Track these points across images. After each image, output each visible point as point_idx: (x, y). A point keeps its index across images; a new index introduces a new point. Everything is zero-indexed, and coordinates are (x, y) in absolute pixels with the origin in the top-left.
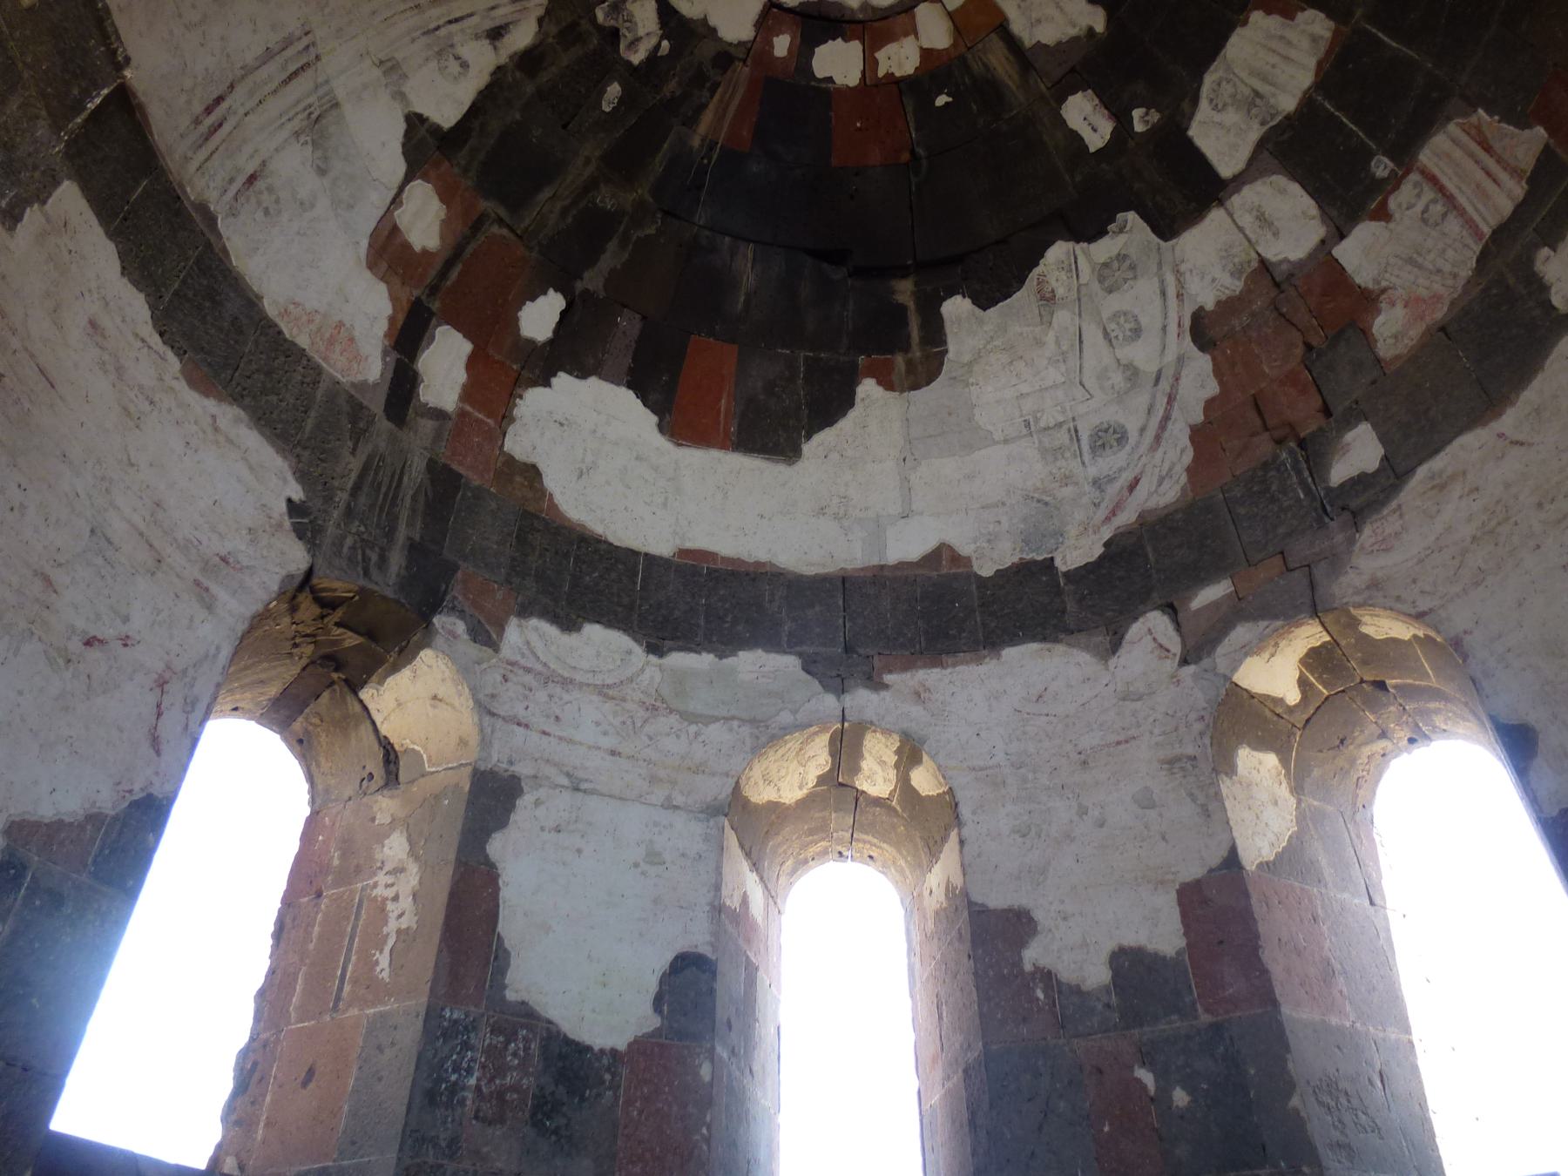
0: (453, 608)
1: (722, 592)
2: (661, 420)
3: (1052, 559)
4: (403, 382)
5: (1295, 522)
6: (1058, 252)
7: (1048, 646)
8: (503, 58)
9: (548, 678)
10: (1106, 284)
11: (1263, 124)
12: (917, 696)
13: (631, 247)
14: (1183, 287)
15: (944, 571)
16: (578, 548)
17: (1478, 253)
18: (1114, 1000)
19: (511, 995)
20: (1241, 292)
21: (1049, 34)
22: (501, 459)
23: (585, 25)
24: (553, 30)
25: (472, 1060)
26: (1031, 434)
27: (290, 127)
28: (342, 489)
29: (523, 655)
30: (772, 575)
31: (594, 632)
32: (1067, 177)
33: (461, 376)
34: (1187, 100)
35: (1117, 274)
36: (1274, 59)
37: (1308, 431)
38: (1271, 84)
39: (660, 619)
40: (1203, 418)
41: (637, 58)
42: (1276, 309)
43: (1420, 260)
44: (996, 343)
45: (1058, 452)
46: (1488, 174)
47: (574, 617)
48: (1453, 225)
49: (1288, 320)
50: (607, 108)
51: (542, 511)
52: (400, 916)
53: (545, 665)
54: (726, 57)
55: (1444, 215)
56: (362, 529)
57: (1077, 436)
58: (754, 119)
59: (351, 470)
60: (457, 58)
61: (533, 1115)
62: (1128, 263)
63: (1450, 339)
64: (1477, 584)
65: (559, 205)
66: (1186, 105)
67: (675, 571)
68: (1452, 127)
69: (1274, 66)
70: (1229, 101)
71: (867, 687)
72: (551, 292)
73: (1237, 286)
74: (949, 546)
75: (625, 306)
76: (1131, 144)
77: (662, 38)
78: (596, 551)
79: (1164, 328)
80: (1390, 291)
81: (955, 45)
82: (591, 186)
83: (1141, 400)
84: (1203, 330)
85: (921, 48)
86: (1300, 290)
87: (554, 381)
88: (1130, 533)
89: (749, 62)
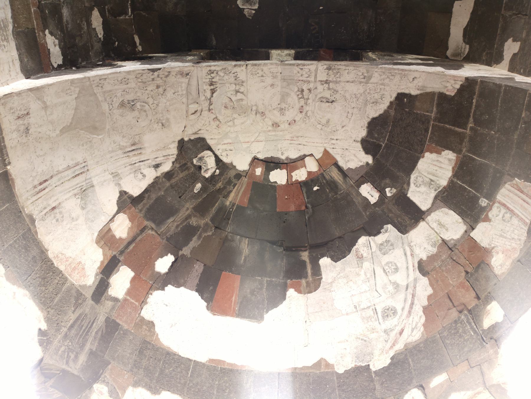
0: (104, 381)
1: (226, 379)
2: (208, 305)
3: (369, 365)
5: (471, 346)
6: (363, 240)
8: (159, 174)
10: (382, 252)
11: (435, 190)
13: (202, 239)
14: (413, 252)
15: (322, 371)
16: (165, 357)
17: (527, 230)
20: (436, 252)
23: (189, 164)
24: (178, 166)
26: (357, 311)
28: (65, 327)
30: (248, 371)
33: (128, 285)
34: (405, 184)
35: (386, 247)
37: (472, 306)
38: (436, 177)
39: (197, 390)
40: (427, 303)
41: (207, 175)
42: (452, 258)
43: (505, 235)
44: (342, 275)
45: (369, 318)
46: (524, 201)
47: (158, 388)
48: (515, 221)
49: (457, 262)
50: (196, 191)
51: (152, 341)
54: (239, 176)
55: (511, 218)
56: (70, 344)
57: (376, 312)
58: (249, 196)
59: (71, 319)
60: (142, 173)
63: (523, 264)
65: (176, 224)
66: (405, 186)
67: (206, 368)
68: (507, 185)
69: (436, 170)
70: (422, 183)
72: (169, 255)
73: (435, 250)
74: (325, 359)
75: (198, 261)
76: (386, 200)
77: (217, 169)
78: (173, 358)
79: (407, 268)
80: (495, 248)
81: (319, 170)
82: (189, 217)
83: (401, 296)
85: (307, 171)
86: (460, 250)
87: (166, 288)
88: (402, 353)
89: (247, 177)
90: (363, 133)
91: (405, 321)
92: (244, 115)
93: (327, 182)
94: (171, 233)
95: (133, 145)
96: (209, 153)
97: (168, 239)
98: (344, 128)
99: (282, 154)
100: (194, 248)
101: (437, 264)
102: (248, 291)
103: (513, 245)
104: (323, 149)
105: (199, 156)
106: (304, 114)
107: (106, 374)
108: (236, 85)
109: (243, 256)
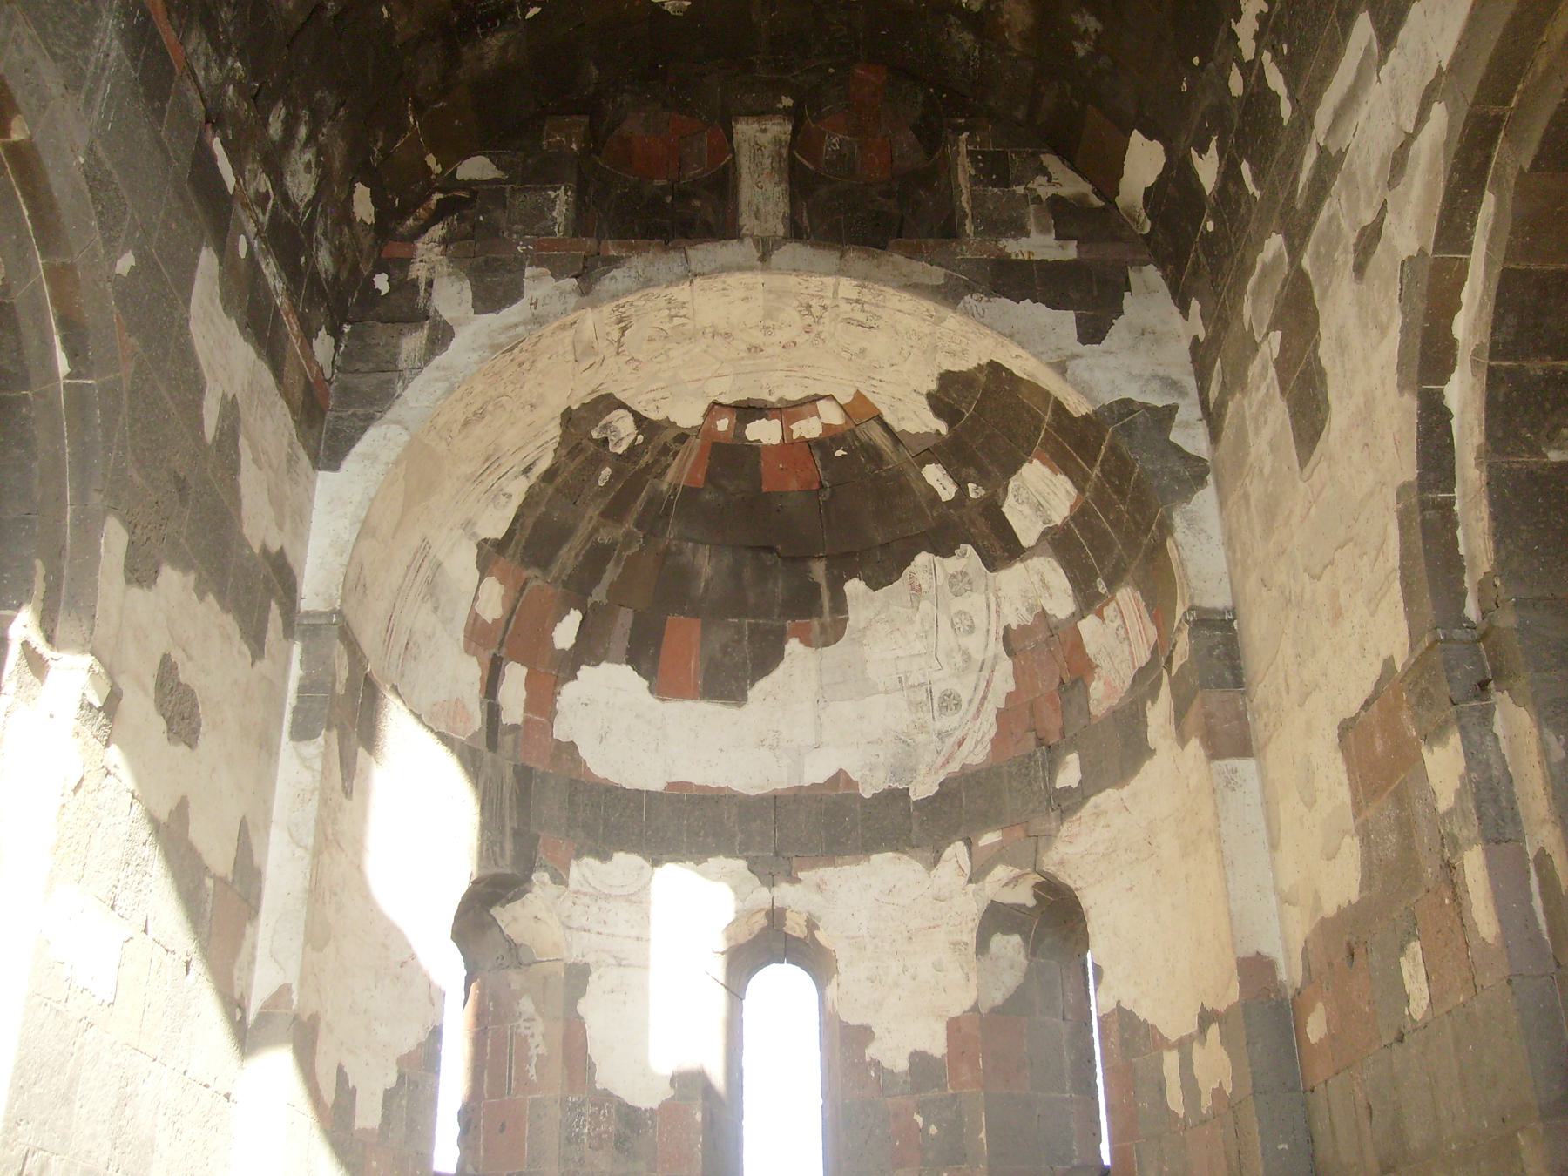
2: (650, 684)
3: (908, 789)
4: (493, 713)
6: (923, 558)
7: (899, 855)
9: (598, 896)
12: (820, 888)
18: (909, 1079)
19: (598, 1086)
21: (912, 426)
22: (554, 744)
23: (585, 442)
24: (564, 452)
25: (585, 1120)
27: (420, 598)
29: (582, 885)
31: (620, 858)
32: (929, 513)
33: (523, 694)
36: (1048, 490)
41: (620, 451)
44: (883, 616)
50: (601, 484)
52: (537, 1046)
53: (594, 888)
54: (683, 437)
61: (615, 1144)
62: (966, 580)
64: (1099, 881)
65: (573, 554)
66: (1000, 490)
71: (788, 882)
72: (572, 611)
73: (1030, 619)
75: (620, 605)
76: (968, 503)
77: (638, 434)
79: (988, 631)
82: (596, 530)
84: (1010, 640)
87: (579, 674)
90: (933, 386)
91: (969, 725)
92: (688, 341)
93: (862, 445)
94: (568, 571)
95: (484, 463)
96: (622, 412)
97: (565, 584)
98: (894, 368)
99: (770, 393)
100: (611, 584)
101: (1030, 644)
102: (717, 646)
103: (1117, 682)
104: (853, 391)
105: (603, 422)
106: (813, 335)
107: (540, 855)
108: (670, 309)
109: (703, 579)
